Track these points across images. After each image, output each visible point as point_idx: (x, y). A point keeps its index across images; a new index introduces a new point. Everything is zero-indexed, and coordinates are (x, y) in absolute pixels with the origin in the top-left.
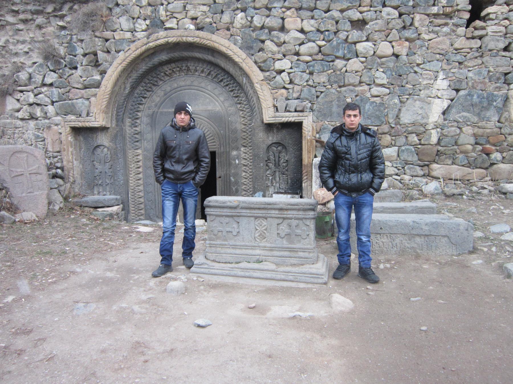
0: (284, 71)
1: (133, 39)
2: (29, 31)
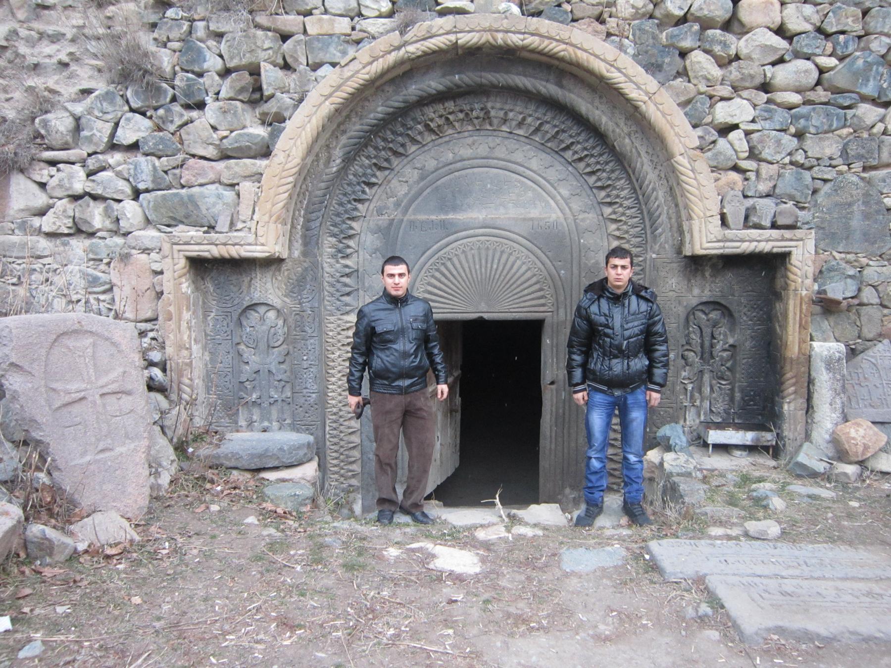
0: (735, 127)
1: (356, 35)
2: (69, 12)
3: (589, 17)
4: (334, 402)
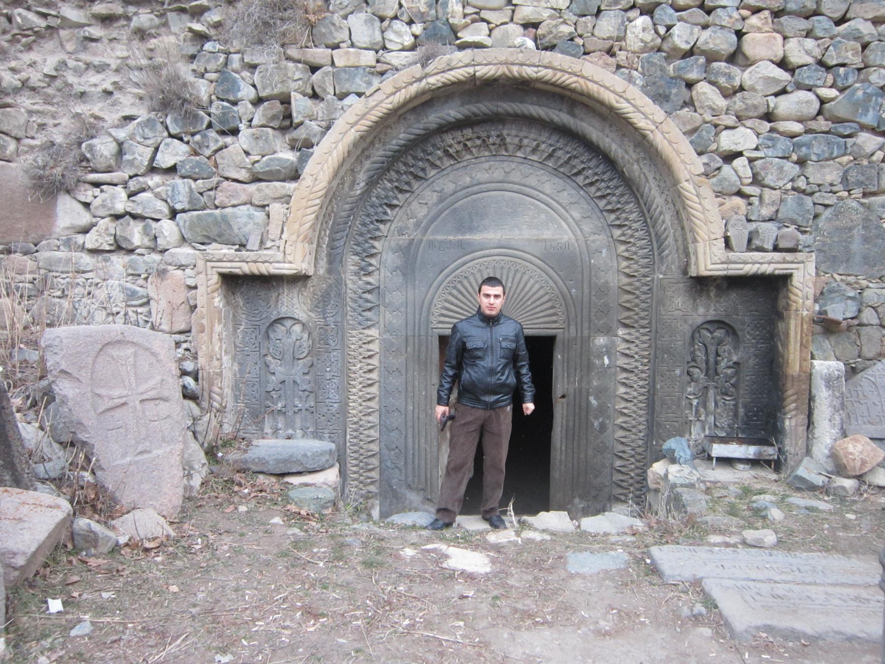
0: (740, 154)
1: (380, 67)
2: (114, 44)
3: (600, 50)
4: (354, 412)
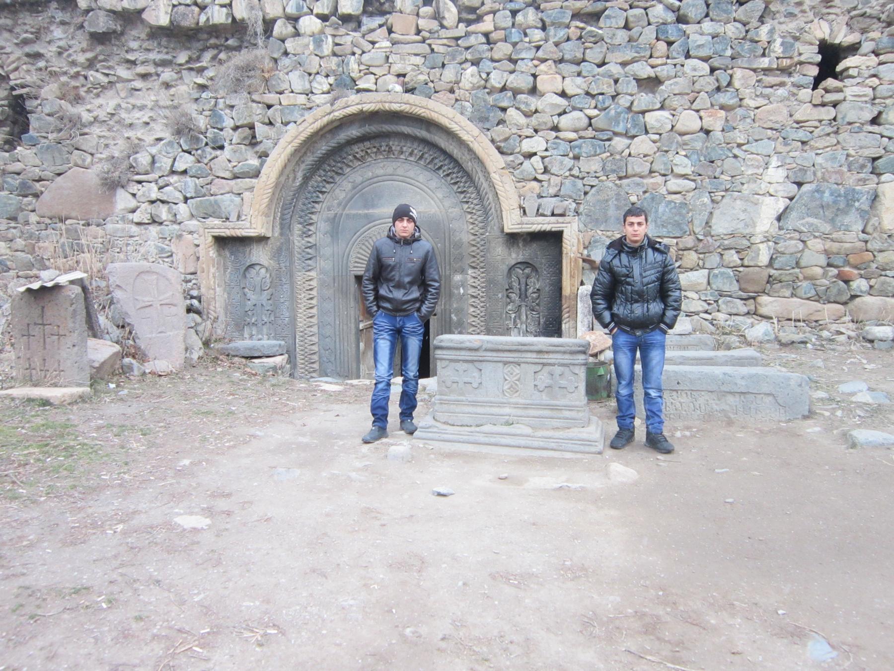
0: (535, 154)
2: (149, 92)
